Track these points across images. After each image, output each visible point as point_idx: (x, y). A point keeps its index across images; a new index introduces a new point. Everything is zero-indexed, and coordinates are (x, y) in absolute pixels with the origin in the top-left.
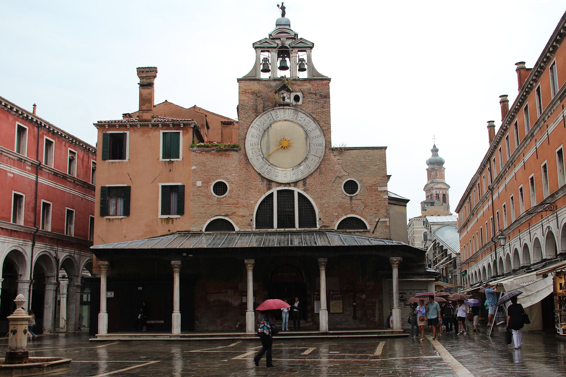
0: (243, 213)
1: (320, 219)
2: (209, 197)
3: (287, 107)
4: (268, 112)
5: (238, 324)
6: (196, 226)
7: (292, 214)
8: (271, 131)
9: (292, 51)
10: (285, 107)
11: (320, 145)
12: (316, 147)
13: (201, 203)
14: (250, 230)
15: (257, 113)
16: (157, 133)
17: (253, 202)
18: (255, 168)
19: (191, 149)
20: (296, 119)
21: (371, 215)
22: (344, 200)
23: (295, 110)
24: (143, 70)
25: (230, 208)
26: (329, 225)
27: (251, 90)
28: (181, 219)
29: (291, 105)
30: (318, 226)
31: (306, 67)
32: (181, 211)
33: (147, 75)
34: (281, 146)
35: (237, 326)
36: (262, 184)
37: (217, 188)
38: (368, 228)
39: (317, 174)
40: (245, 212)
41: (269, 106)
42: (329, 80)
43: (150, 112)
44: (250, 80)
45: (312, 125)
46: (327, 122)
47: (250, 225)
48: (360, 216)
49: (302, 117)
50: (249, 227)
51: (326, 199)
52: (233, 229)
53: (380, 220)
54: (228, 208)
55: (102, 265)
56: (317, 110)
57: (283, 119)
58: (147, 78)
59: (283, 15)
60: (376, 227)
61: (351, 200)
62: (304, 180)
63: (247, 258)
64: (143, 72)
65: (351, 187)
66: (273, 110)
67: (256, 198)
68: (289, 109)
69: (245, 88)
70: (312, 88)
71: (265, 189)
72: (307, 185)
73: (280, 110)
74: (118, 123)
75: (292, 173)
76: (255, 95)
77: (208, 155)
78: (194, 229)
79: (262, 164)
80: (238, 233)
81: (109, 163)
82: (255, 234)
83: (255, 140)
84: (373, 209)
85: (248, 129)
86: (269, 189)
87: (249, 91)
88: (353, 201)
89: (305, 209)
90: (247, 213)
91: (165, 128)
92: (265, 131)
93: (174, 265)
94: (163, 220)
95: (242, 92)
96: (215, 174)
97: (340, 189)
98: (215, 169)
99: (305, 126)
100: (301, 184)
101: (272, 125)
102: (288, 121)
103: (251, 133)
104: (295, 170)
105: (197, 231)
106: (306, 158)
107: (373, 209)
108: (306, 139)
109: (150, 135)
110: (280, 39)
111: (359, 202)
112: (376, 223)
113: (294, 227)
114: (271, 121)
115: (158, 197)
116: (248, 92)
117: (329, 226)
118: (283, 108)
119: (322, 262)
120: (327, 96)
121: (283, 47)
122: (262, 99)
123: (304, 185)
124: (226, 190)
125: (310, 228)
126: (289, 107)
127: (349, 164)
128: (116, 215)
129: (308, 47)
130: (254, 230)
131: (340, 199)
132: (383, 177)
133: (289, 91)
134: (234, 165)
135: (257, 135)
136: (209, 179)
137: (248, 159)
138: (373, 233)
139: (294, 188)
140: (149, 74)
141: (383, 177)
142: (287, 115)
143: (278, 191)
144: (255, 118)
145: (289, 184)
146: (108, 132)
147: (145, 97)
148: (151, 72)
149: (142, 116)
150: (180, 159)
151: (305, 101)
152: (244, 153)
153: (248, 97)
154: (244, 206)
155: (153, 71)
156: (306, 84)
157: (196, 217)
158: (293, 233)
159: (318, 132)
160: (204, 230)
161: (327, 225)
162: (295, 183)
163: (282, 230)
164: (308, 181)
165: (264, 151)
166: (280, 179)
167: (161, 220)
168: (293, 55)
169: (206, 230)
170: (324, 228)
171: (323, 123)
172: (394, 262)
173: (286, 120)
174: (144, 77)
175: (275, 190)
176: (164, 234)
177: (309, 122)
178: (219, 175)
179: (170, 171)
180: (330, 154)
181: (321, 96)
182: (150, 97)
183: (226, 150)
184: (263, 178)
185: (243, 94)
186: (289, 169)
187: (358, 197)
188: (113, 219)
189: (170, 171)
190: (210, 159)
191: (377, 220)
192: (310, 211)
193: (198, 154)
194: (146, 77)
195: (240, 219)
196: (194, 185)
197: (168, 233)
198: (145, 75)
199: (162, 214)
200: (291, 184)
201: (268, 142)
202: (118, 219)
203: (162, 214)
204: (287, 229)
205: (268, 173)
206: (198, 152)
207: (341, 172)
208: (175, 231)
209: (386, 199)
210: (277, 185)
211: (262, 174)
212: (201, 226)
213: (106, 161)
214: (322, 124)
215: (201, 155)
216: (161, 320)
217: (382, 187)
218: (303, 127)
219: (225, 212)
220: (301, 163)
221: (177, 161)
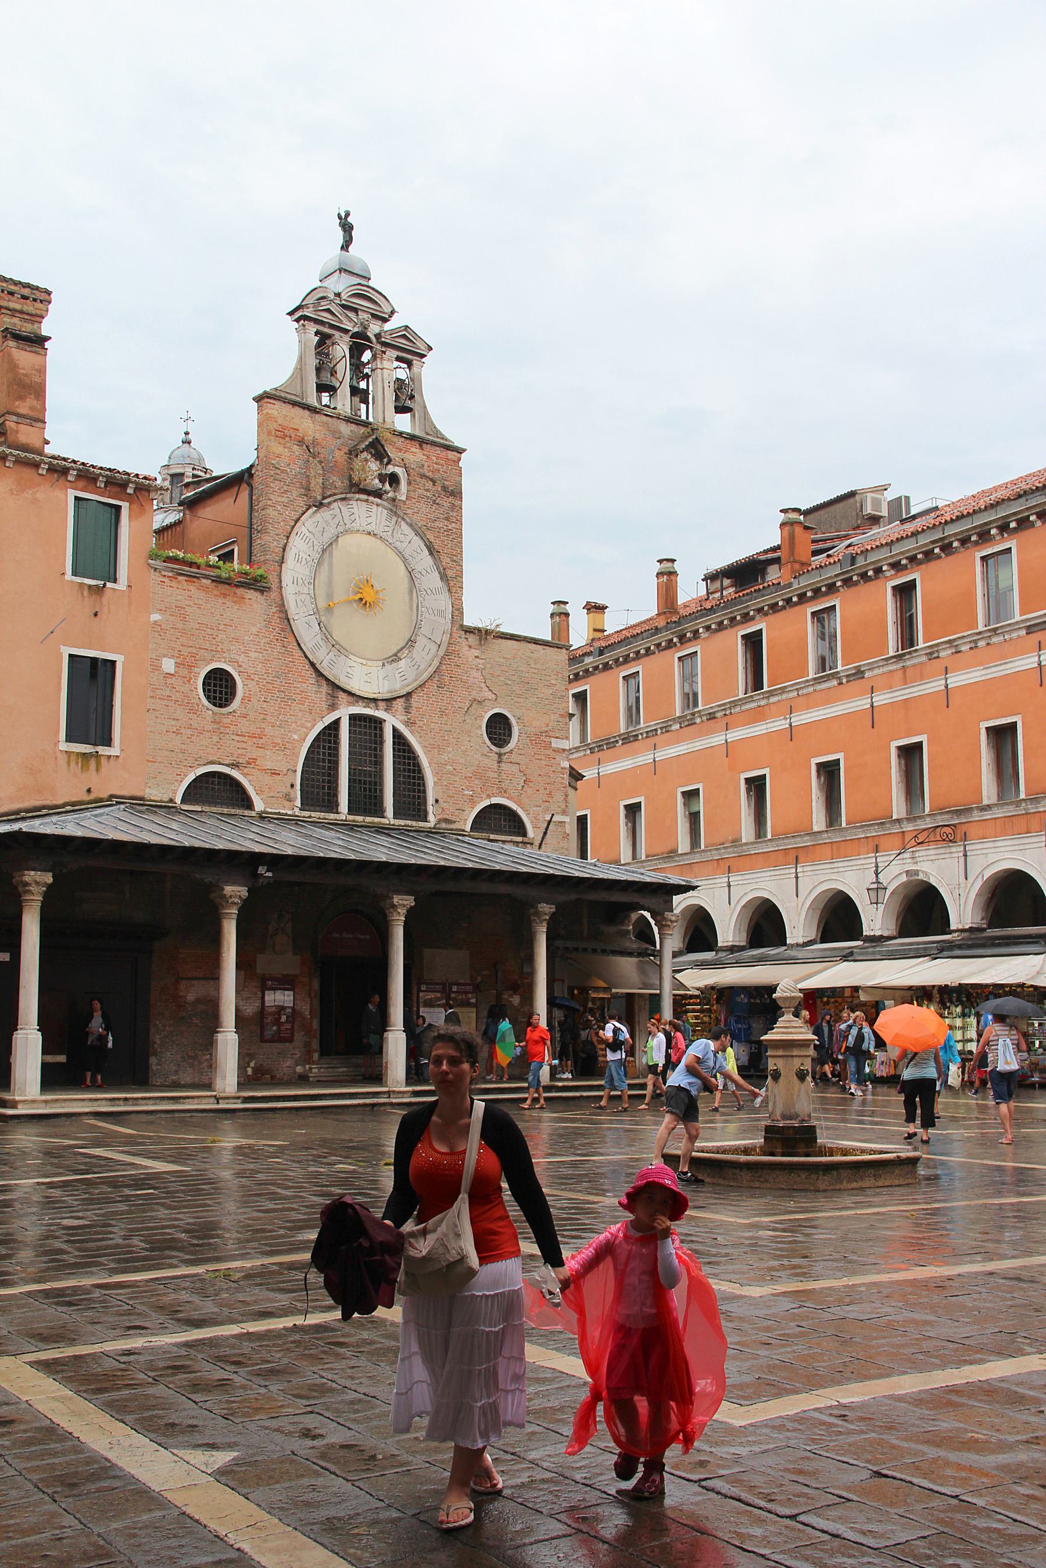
0: (274, 764)
1: (437, 801)
5: (252, 1064)
6: (158, 785)
9: (384, 352)
10: (371, 498)
11: (441, 613)
12: (432, 617)
13: (174, 722)
14: (290, 812)
16: (58, 493)
17: (295, 737)
21: (538, 803)
22: (486, 761)
23: (391, 510)
24: (13, 288)
28: (120, 760)
30: (431, 818)
33: (25, 308)
38: (531, 833)
39: (432, 687)
40: (278, 761)
42: (460, 451)
44: (294, 404)
45: (424, 561)
47: (289, 798)
48: (515, 802)
50: (287, 803)
51: (449, 752)
52: (248, 804)
54: (239, 745)
55: (37, 883)
56: (437, 524)
58: (26, 317)
59: (345, 247)
60: (545, 833)
61: (499, 762)
62: (409, 695)
63: (399, 892)
64: (12, 294)
69: (280, 421)
70: (426, 465)
72: (413, 711)
73: (359, 502)
75: (382, 673)
76: (304, 447)
77: (192, 588)
78: (155, 793)
80: (262, 817)
82: (296, 821)
84: (542, 791)
85: (288, 537)
86: (333, 707)
88: (502, 765)
89: (404, 769)
90: (282, 766)
91: (81, 484)
92: (324, 551)
93: (231, 897)
94: (73, 758)
96: (208, 646)
98: (210, 631)
104: (388, 667)
105: (161, 801)
106: (411, 642)
107: (542, 791)
108: (411, 592)
110: (356, 311)
112: (546, 825)
114: (341, 529)
115: (60, 689)
117: (455, 822)
118: (367, 501)
119: (545, 914)
120: (456, 493)
122: (321, 462)
123: (407, 709)
127: (498, 673)
130: (297, 812)
131: (478, 756)
132: (561, 716)
134: (254, 630)
135: (309, 559)
136: (193, 655)
137: (288, 620)
138: (540, 847)
139: (385, 713)
140: (29, 307)
141: (561, 716)
143: (353, 718)
147: (24, 375)
148: (35, 300)
149: (17, 432)
150: (122, 584)
155: (41, 301)
156: (414, 450)
157: (159, 759)
158: (381, 830)
159: (434, 580)
160: (178, 800)
161: (449, 817)
163: (360, 818)
166: (356, 685)
167: (65, 756)
170: (444, 825)
172: (669, 923)
173: (369, 534)
174: (15, 310)
175: (344, 712)
178: (219, 649)
179: (96, 615)
180: (461, 640)
181: (445, 488)
182: (38, 380)
185: (277, 436)
187: (514, 757)
189: (96, 615)
193: (166, 580)
194: (22, 312)
195: (268, 779)
196: (157, 668)
198: (18, 307)
199: (69, 739)
200: (381, 704)
201: (330, 582)
203: (69, 739)
204: (369, 819)
206: (166, 574)
208: (104, 795)
209: (565, 768)
210: (351, 699)
211: (318, 666)
214: (446, 560)
218: (404, 560)
219: (232, 755)
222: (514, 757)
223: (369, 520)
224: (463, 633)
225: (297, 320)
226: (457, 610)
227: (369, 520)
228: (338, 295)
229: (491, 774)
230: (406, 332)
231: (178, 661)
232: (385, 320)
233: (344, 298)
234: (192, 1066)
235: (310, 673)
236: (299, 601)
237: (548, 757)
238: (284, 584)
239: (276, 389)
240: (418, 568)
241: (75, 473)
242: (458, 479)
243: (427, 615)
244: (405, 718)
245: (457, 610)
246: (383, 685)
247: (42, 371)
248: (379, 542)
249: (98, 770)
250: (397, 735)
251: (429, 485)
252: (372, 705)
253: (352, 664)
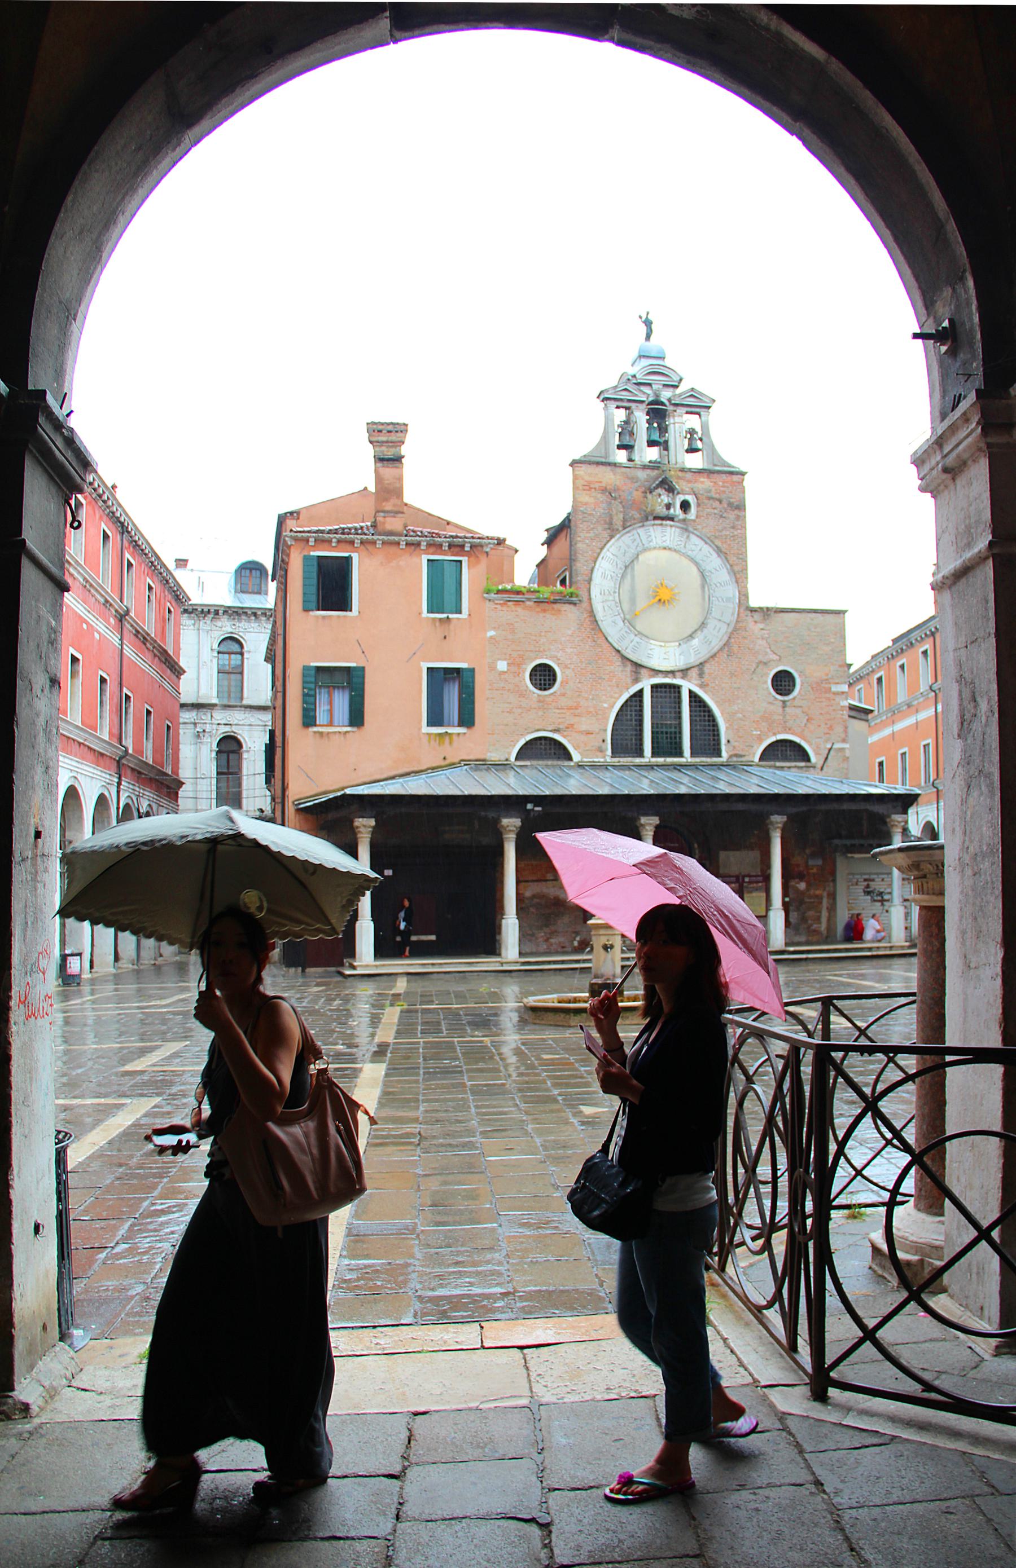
1: (728, 741)
2: (522, 694)
3: (669, 522)
4: (633, 529)
5: (578, 939)
7: (677, 730)
8: (637, 567)
9: (675, 411)
10: (664, 522)
11: (729, 600)
13: (507, 705)
14: (602, 760)
15: (613, 532)
16: (415, 559)
17: (605, 705)
18: (609, 639)
19: (485, 595)
20: (685, 547)
22: (772, 707)
23: (682, 528)
24: (381, 427)
25: (563, 716)
26: (743, 753)
27: (600, 485)
28: (467, 735)
29: (676, 519)
30: (724, 754)
31: (699, 445)
32: (467, 719)
33: (390, 439)
34: (657, 598)
35: (576, 944)
36: (622, 671)
37: (536, 675)
38: (813, 759)
39: (724, 655)
41: (634, 519)
42: (743, 474)
43: (400, 515)
44: (598, 463)
45: (713, 562)
46: (741, 556)
47: (601, 750)
48: (799, 736)
49: (697, 546)
50: (599, 754)
52: (569, 757)
53: (835, 746)
54: (559, 716)
56: (724, 533)
57: (661, 545)
60: (826, 758)
61: (784, 707)
62: (701, 665)
64: (380, 431)
65: (783, 682)
66: (643, 526)
67: (612, 697)
68: (671, 526)
69: (587, 478)
70: (713, 490)
71: (629, 680)
72: (706, 677)
73: (655, 527)
74: (337, 536)
75: (678, 651)
77: (519, 609)
78: (494, 756)
79: (623, 632)
80: (580, 766)
81: (317, 617)
83: (609, 585)
84: (823, 726)
85: (595, 562)
86: (636, 680)
87: (597, 486)
88: (787, 709)
89: (700, 720)
91: (432, 550)
92: (626, 567)
94: (433, 737)
95: (579, 486)
97: (765, 686)
98: (534, 638)
99: (701, 562)
100: (694, 673)
101: (640, 557)
102: (670, 549)
103: (601, 570)
104: (684, 646)
106: (703, 625)
108: (703, 587)
109: (402, 563)
110: (650, 385)
111: (798, 711)
112: (827, 752)
113: (680, 754)
114: (639, 549)
116: (595, 488)
117: (744, 756)
118: (661, 525)
120: (739, 507)
121: (657, 402)
123: (701, 675)
124: (555, 680)
125: (711, 757)
126: (671, 523)
128: (331, 724)
129: (698, 405)
130: (608, 759)
133: (671, 490)
134: (569, 632)
135: (613, 574)
136: (521, 656)
138: (822, 769)
140: (393, 437)
141: (840, 666)
142: (667, 538)
143: (654, 688)
144: (608, 541)
145: (672, 673)
146: (312, 553)
147: (388, 484)
148: (397, 432)
149: (384, 523)
150: (464, 615)
151: (701, 513)
152: (588, 608)
153: (595, 498)
154: (591, 712)
156: (702, 479)
160: (513, 758)
161: (740, 753)
162: (684, 672)
164: (707, 669)
165: (626, 606)
166: (655, 663)
168: (677, 419)
169: (517, 759)
170: (735, 759)
171: (735, 558)
173: (665, 548)
174: (383, 442)
175: (646, 684)
176: (434, 765)
177: (709, 555)
179: (445, 638)
180: (748, 618)
181: (730, 504)
182: (398, 485)
183: (555, 602)
184: (625, 658)
186: (673, 644)
187: (796, 703)
188: (328, 733)
189: (445, 638)
190: (522, 618)
191: (829, 746)
192: (709, 725)
194: (387, 442)
195: (584, 738)
196: (493, 668)
197: (443, 763)
198: (384, 439)
202: (340, 732)
205: (634, 650)
207: (766, 653)
208: (456, 760)
210: (652, 673)
211: (623, 652)
212: (508, 750)
213: (311, 613)
214: (733, 559)
215: (505, 608)
216: (431, 934)
217: (838, 686)
218: (696, 564)
219: (554, 723)
220: (694, 633)
221: (458, 619)
222: (796, 703)
223: (664, 539)
224: (749, 612)
225: (603, 401)
226: (744, 595)
227: (664, 539)
228: (634, 376)
229: (776, 717)
230: (693, 393)
231: (510, 662)
232: (676, 387)
233: (640, 377)
234: (530, 941)
235: (617, 660)
236: (606, 608)
237: (829, 699)
238: (593, 596)
239: (585, 456)
240: (708, 568)
241: (425, 544)
242: (741, 495)
243: (717, 603)
244: (700, 682)
245: (744, 595)
246: (680, 659)
247: (400, 479)
248: (674, 554)
249: (451, 743)
250: (692, 695)
252: (670, 675)
253: (653, 647)
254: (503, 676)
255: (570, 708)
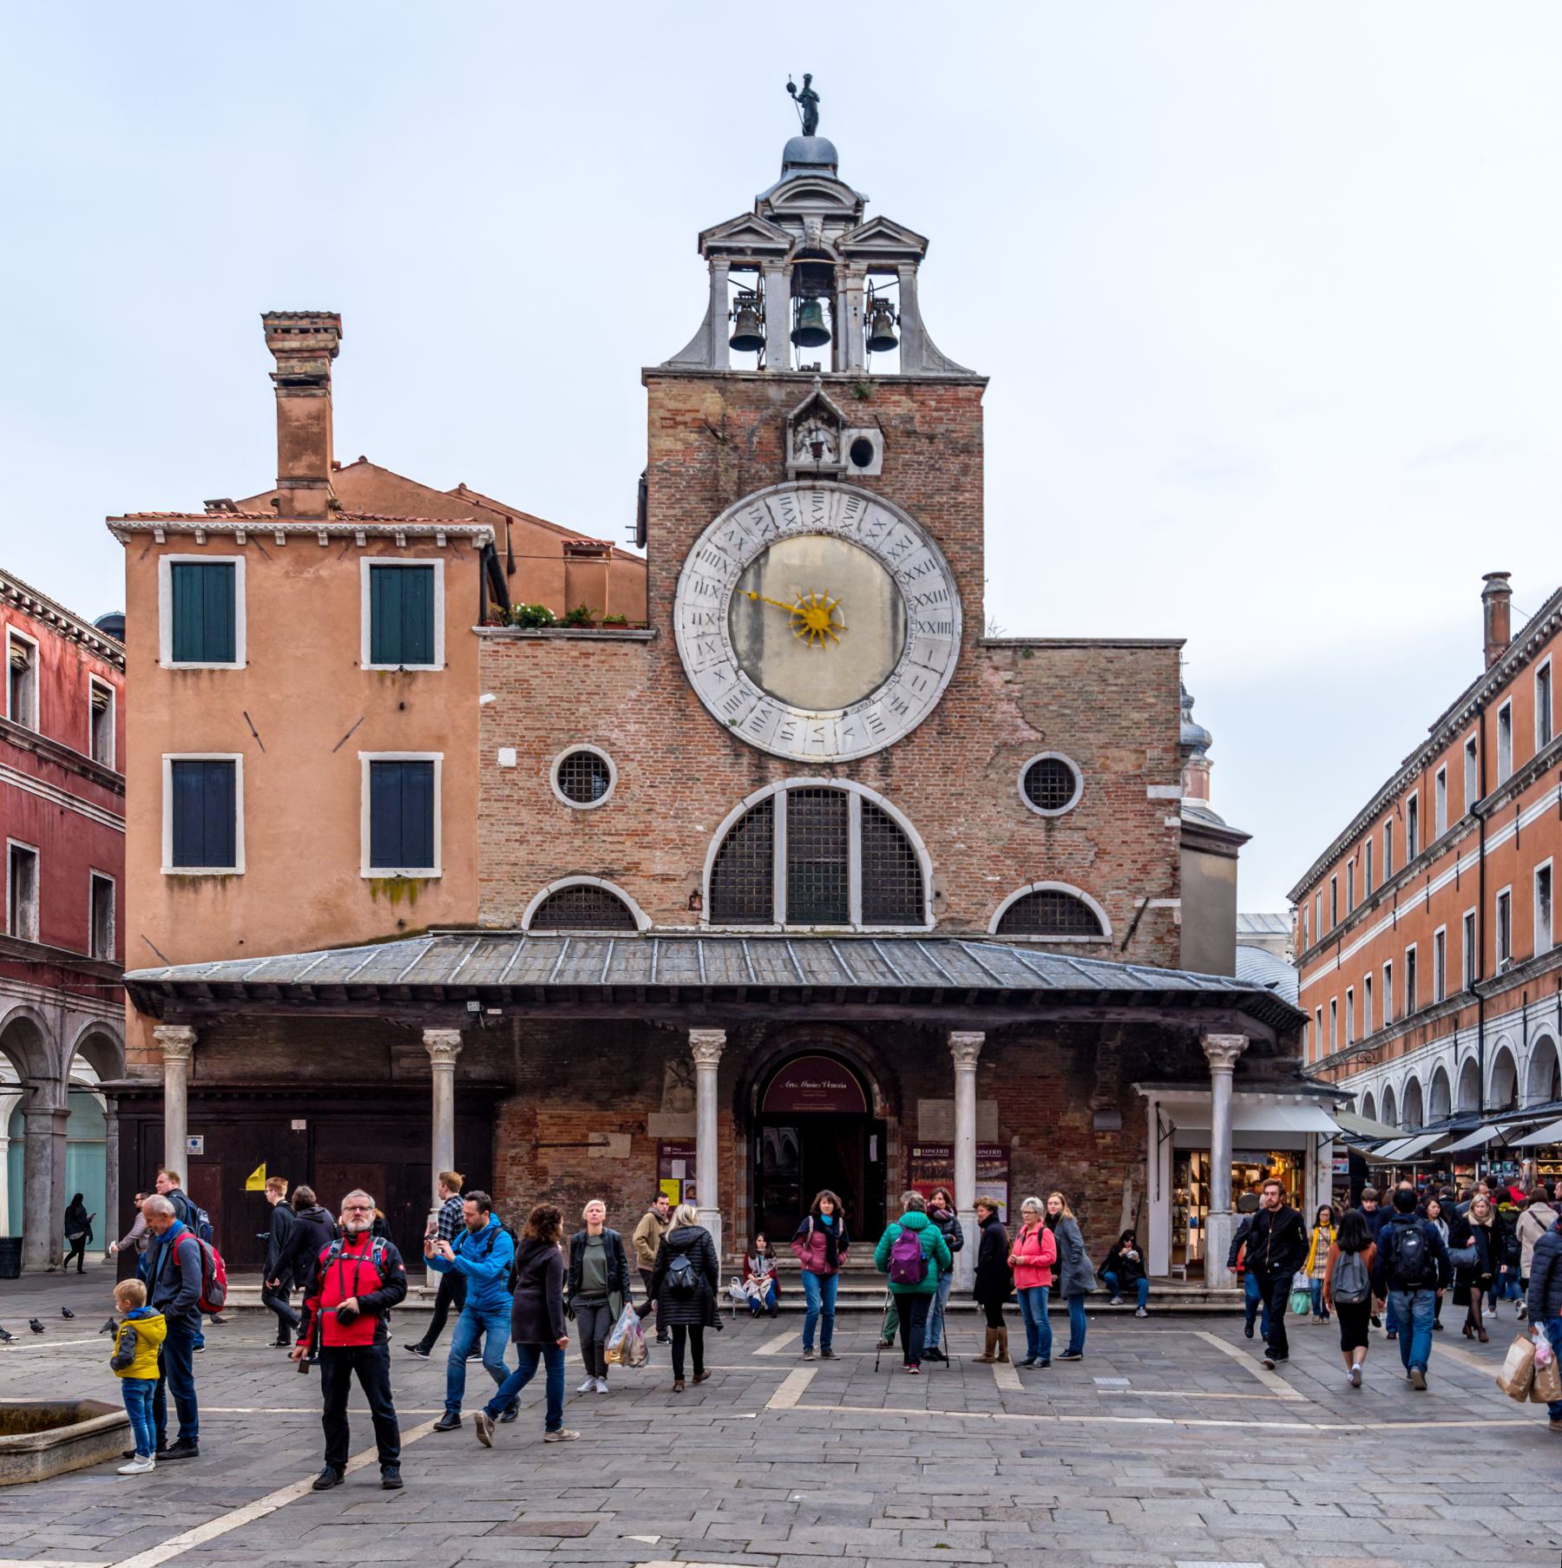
13: (516, 829)
28: (442, 882)
71: (745, 781)
86: (761, 781)
118: (813, 488)
123: (885, 771)
138: (1124, 947)
143: (793, 794)
145: (830, 767)
160: (525, 925)
175: (778, 787)
196: (489, 761)
251: (923, 444)
254: (508, 776)
255: (633, 834)
